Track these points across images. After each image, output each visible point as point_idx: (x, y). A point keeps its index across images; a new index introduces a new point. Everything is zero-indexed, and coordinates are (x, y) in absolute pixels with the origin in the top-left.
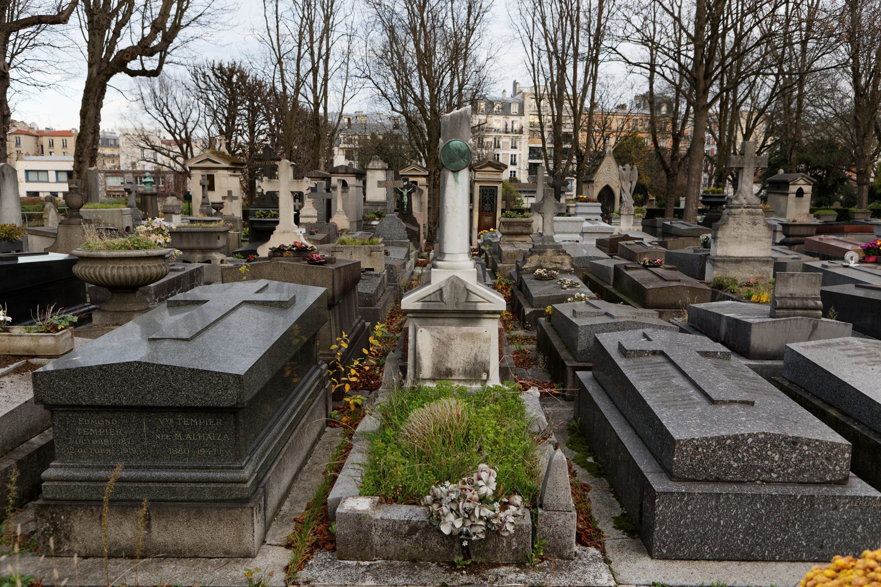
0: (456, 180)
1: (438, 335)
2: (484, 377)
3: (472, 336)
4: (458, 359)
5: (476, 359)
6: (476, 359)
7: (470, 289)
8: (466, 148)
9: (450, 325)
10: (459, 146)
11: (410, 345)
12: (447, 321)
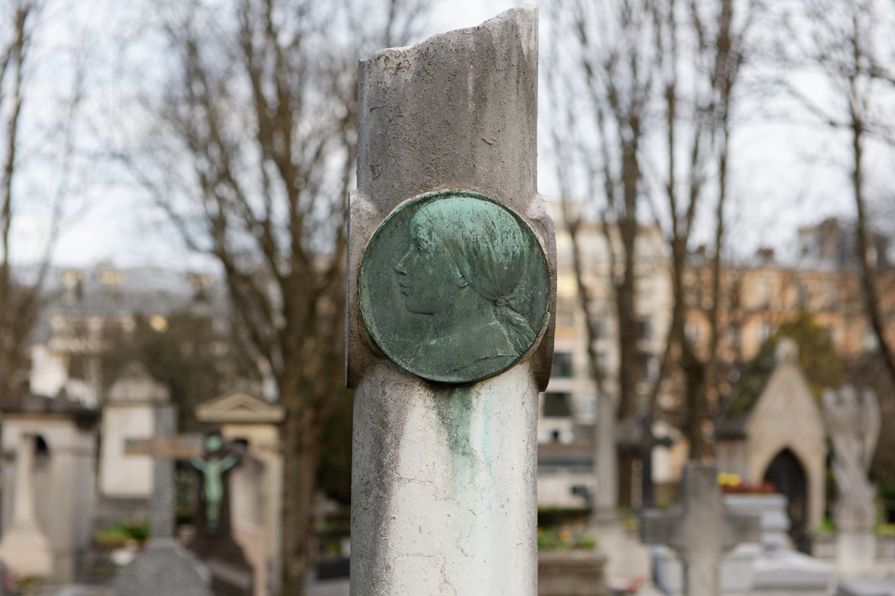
0: (457, 444)
8: (517, 243)
10: (474, 229)
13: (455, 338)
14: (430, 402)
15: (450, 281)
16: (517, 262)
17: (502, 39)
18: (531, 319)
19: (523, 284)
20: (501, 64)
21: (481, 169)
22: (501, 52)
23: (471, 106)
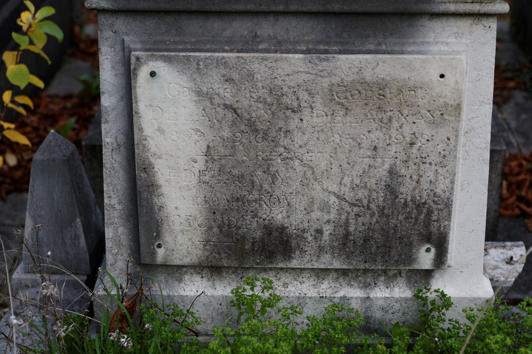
1: (227, 93)
2: (425, 258)
3: (378, 97)
4: (317, 192)
5: (392, 191)
6: (392, 191)
9: (282, 46)
11: (110, 133)
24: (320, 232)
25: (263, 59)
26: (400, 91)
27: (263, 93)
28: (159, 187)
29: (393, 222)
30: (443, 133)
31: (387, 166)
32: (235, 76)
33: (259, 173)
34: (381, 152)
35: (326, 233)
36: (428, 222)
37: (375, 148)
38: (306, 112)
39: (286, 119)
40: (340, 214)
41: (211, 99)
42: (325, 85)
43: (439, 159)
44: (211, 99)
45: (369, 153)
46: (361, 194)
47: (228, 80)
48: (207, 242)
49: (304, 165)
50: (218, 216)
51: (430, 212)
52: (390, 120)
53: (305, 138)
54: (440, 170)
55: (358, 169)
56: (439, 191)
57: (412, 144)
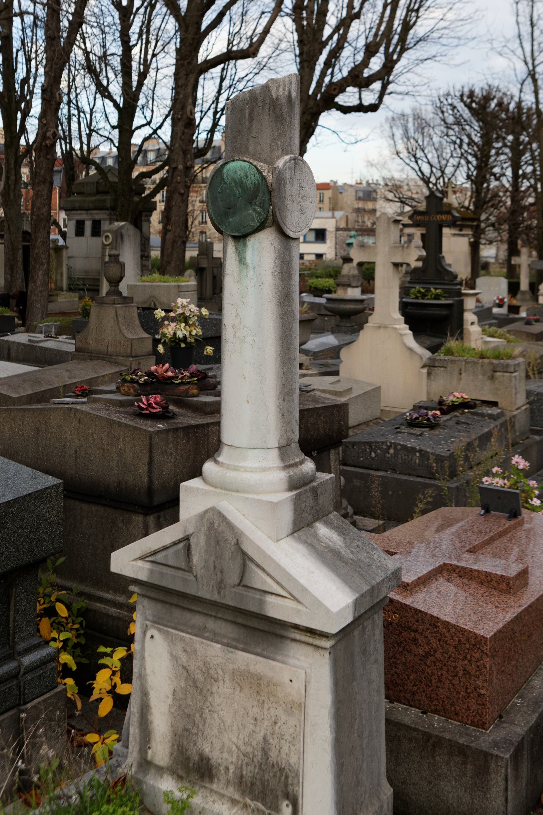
0: (242, 260)
1: (184, 658)
6: (265, 753)
7: (250, 552)
8: (256, 178)
9: (215, 638)
10: (241, 174)
12: (211, 624)
13: (237, 218)
14: (233, 244)
15: (235, 195)
16: (257, 187)
17: (260, 93)
18: (264, 209)
19: (260, 195)
20: (260, 104)
21: (251, 148)
22: (260, 98)
23: (247, 123)
24: (227, 768)
25: (202, 643)
26: (268, 684)
27: (201, 664)
28: (151, 708)
29: (267, 776)
30: (292, 721)
31: (262, 734)
32: (188, 650)
33: (197, 715)
34: (259, 722)
35: (231, 771)
36: (286, 785)
37: (256, 719)
38: (221, 683)
39: (211, 684)
40: (238, 760)
41: (177, 660)
42: (231, 669)
43: (291, 739)
44: (177, 660)
45: (253, 721)
46: (249, 749)
47: (185, 651)
48: (172, 754)
49: (220, 719)
50: (177, 738)
51: (287, 777)
52: (263, 702)
53: (221, 699)
54: (292, 747)
55: (247, 731)
56: (292, 762)
57: (276, 723)
